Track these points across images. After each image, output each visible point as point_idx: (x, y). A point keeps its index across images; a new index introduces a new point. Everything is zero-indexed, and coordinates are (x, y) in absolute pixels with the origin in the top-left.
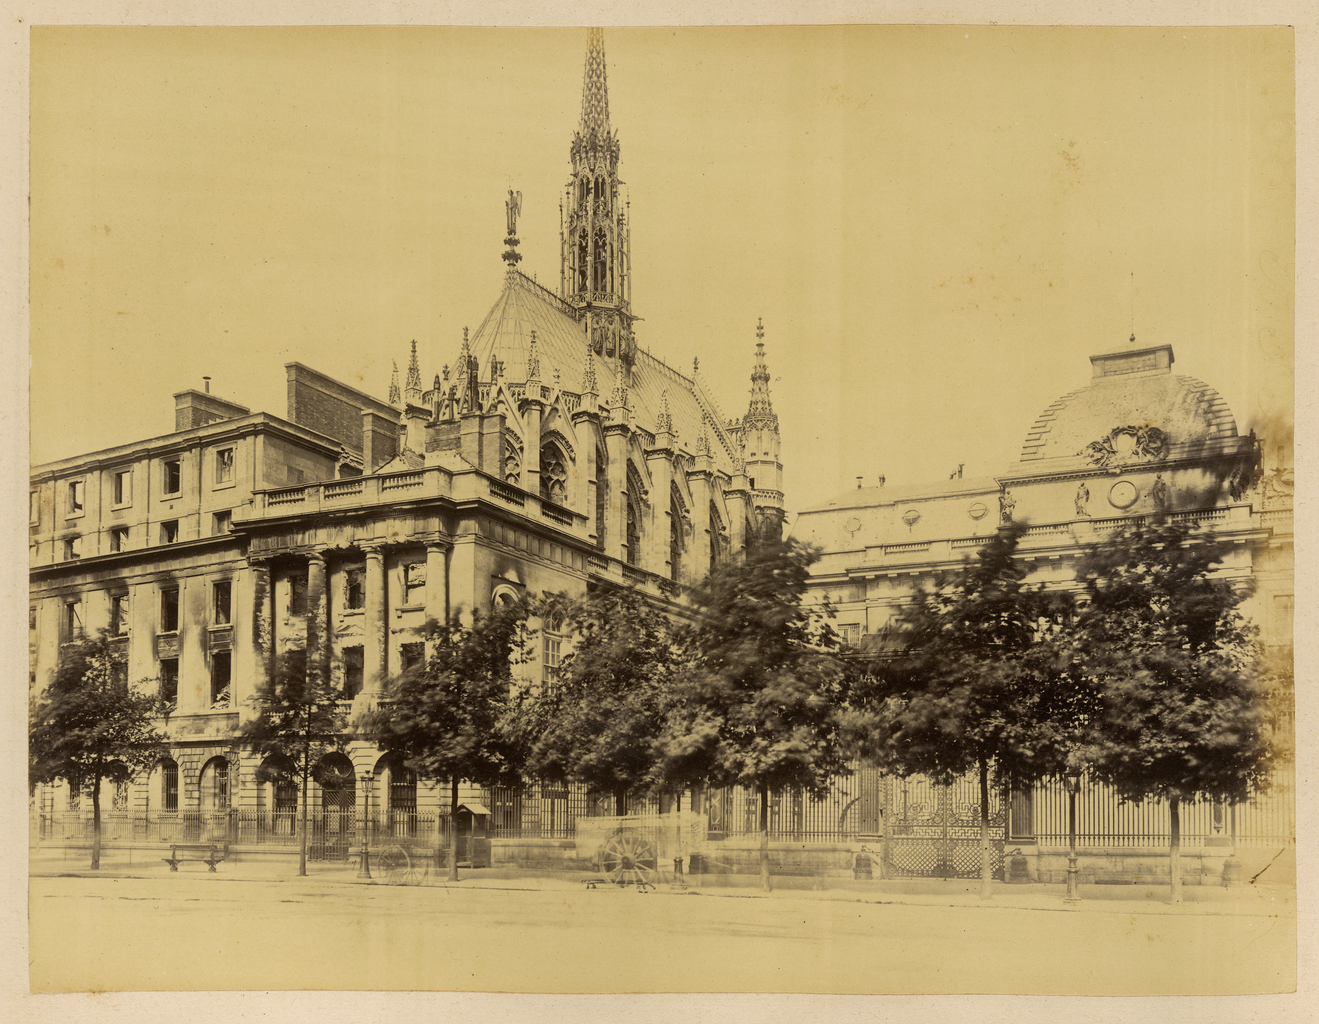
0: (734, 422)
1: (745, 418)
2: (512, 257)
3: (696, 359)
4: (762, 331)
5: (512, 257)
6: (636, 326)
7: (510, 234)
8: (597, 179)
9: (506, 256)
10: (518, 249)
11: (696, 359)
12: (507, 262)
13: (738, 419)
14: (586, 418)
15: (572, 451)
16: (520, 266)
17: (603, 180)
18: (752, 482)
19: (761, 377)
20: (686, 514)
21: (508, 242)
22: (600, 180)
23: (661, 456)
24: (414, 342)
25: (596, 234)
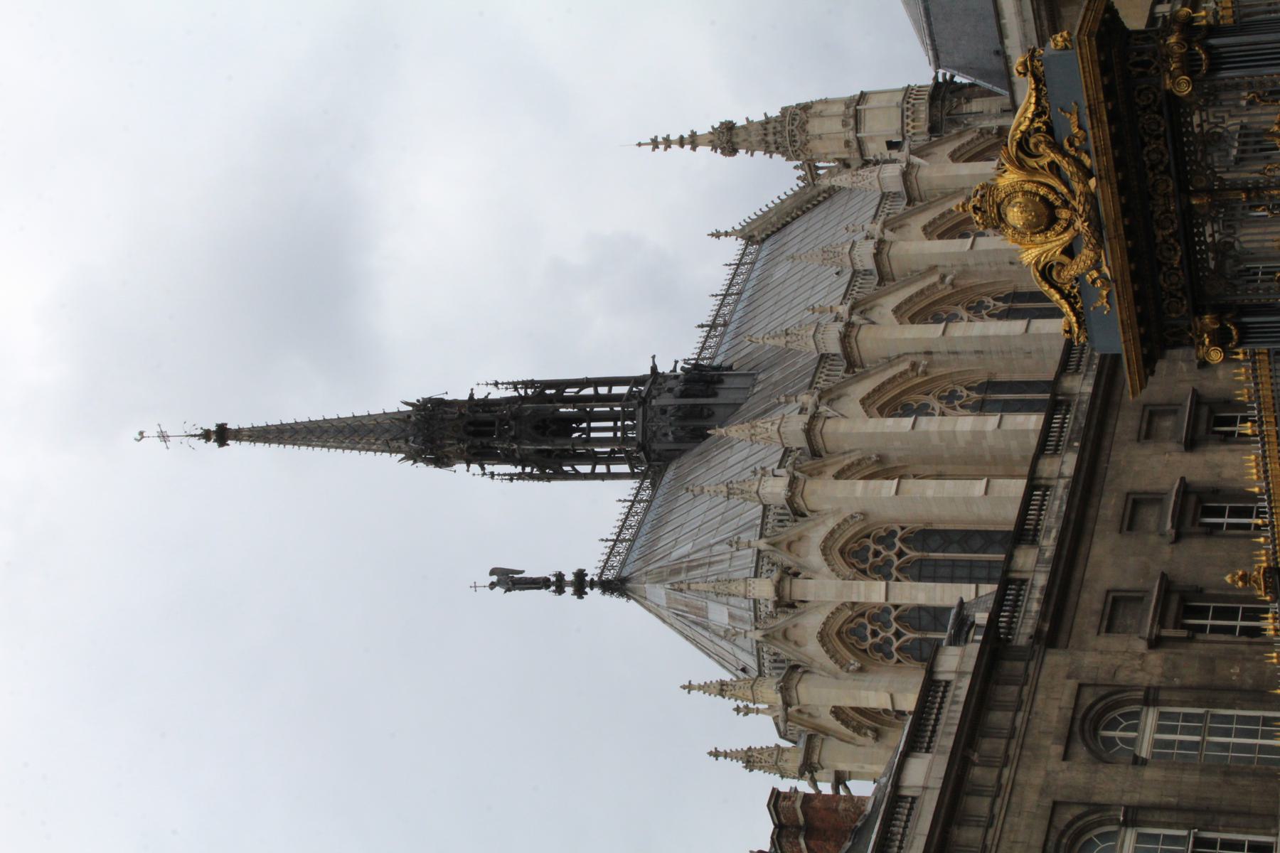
0: (801, 173)
1: (789, 159)
2: (581, 584)
3: (712, 235)
4: (660, 139)
5: (581, 584)
6: (665, 367)
7: (548, 587)
8: (469, 434)
9: (580, 593)
10: (569, 577)
11: (712, 235)
12: (588, 590)
13: (796, 167)
14: (799, 500)
15: (852, 517)
16: (592, 573)
17: (470, 424)
18: (891, 145)
19: (727, 139)
20: (948, 279)
21: (560, 590)
22: (472, 428)
23: (854, 344)
24: (716, 754)
25: (543, 434)
